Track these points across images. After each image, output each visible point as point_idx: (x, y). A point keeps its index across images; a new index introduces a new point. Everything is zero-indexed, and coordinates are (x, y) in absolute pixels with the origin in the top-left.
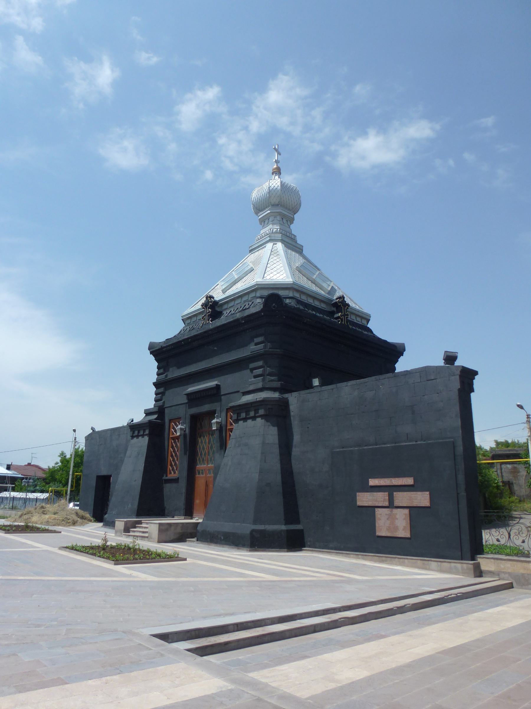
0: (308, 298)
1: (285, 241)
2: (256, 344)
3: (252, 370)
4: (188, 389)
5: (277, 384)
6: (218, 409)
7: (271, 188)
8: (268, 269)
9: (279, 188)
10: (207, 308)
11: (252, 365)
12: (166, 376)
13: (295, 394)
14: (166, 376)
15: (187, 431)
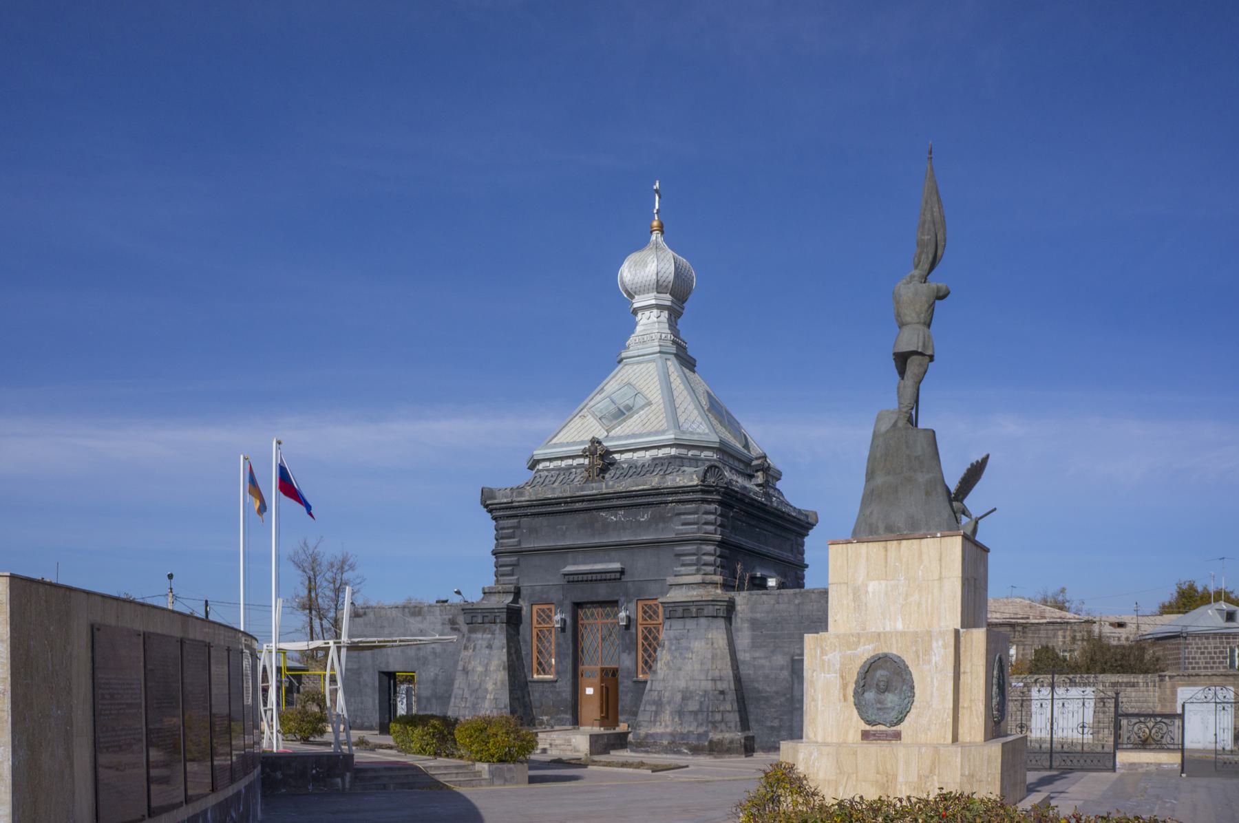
0: (730, 458)
1: (679, 356)
2: (684, 524)
3: (678, 555)
4: (565, 567)
5: (718, 578)
6: (622, 599)
7: (660, 275)
8: (679, 412)
9: (672, 277)
10: (593, 458)
11: (679, 549)
12: (519, 542)
13: (744, 594)
14: (519, 542)
15: (569, 621)
